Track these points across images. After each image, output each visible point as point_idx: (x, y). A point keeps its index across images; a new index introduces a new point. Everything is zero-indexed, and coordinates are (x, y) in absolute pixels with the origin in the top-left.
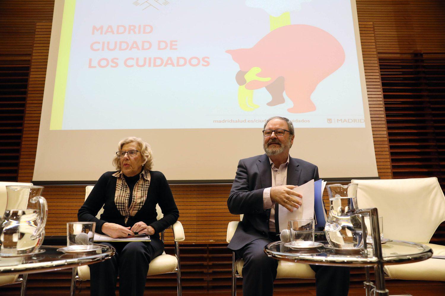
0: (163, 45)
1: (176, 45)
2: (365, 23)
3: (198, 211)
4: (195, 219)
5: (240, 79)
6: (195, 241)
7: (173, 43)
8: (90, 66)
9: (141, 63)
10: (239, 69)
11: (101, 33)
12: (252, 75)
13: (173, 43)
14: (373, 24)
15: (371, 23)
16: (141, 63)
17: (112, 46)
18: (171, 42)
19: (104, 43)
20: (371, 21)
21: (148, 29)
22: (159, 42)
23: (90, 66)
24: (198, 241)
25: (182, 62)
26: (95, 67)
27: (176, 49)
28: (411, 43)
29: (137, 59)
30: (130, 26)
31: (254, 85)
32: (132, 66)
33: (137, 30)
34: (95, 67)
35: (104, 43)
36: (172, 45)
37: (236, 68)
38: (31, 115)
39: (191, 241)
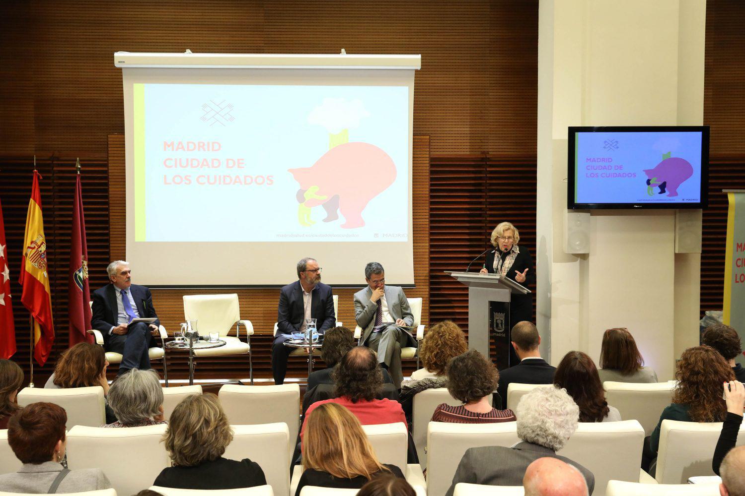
0: (231, 163)
1: (243, 163)
2: (422, 137)
3: (265, 309)
4: (262, 315)
5: (300, 197)
6: (262, 333)
7: (241, 161)
8: (166, 183)
9: (212, 181)
10: (300, 188)
11: (173, 150)
12: (310, 194)
13: (241, 161)
14: (429, 139)
15: (428, 137)
16: (212, 181)
17: (184, 164)
18: (239, 160)
19: (176, 160)
20: (428, 135)
21: (216, 146)
22: (228, 160)
23: (166, 183)
24: (265, 333)
25: (249, 180)
26: (170, 184)
27: (243, 167)
28: (483, 141)
29: (208, 177)
30: (199, 143)
31: (313, 203)
32: (204, 183)
33: (206, 147)
34: (170, 184)
35: (176, 160)
36: (239, 163)
37: (297, 187)
38: (115, 227)
39: (258, 333)
